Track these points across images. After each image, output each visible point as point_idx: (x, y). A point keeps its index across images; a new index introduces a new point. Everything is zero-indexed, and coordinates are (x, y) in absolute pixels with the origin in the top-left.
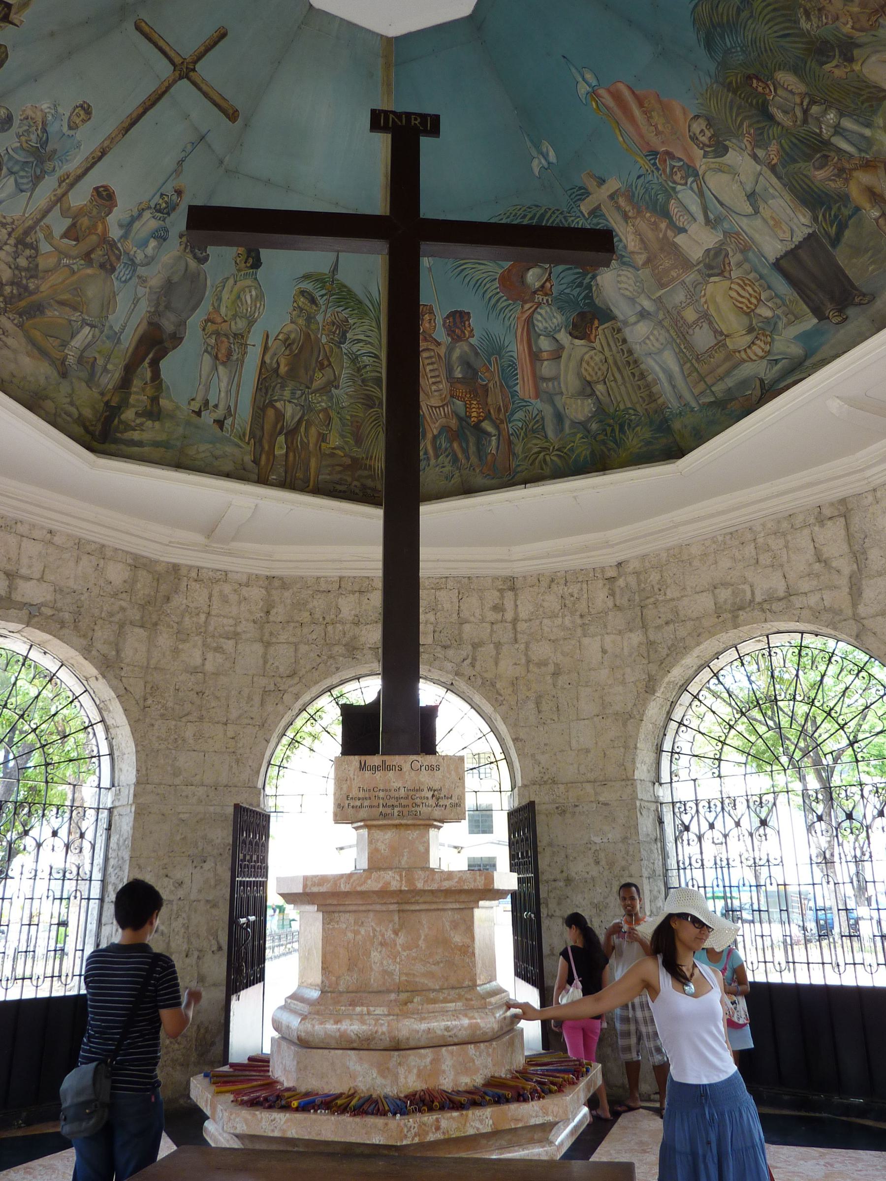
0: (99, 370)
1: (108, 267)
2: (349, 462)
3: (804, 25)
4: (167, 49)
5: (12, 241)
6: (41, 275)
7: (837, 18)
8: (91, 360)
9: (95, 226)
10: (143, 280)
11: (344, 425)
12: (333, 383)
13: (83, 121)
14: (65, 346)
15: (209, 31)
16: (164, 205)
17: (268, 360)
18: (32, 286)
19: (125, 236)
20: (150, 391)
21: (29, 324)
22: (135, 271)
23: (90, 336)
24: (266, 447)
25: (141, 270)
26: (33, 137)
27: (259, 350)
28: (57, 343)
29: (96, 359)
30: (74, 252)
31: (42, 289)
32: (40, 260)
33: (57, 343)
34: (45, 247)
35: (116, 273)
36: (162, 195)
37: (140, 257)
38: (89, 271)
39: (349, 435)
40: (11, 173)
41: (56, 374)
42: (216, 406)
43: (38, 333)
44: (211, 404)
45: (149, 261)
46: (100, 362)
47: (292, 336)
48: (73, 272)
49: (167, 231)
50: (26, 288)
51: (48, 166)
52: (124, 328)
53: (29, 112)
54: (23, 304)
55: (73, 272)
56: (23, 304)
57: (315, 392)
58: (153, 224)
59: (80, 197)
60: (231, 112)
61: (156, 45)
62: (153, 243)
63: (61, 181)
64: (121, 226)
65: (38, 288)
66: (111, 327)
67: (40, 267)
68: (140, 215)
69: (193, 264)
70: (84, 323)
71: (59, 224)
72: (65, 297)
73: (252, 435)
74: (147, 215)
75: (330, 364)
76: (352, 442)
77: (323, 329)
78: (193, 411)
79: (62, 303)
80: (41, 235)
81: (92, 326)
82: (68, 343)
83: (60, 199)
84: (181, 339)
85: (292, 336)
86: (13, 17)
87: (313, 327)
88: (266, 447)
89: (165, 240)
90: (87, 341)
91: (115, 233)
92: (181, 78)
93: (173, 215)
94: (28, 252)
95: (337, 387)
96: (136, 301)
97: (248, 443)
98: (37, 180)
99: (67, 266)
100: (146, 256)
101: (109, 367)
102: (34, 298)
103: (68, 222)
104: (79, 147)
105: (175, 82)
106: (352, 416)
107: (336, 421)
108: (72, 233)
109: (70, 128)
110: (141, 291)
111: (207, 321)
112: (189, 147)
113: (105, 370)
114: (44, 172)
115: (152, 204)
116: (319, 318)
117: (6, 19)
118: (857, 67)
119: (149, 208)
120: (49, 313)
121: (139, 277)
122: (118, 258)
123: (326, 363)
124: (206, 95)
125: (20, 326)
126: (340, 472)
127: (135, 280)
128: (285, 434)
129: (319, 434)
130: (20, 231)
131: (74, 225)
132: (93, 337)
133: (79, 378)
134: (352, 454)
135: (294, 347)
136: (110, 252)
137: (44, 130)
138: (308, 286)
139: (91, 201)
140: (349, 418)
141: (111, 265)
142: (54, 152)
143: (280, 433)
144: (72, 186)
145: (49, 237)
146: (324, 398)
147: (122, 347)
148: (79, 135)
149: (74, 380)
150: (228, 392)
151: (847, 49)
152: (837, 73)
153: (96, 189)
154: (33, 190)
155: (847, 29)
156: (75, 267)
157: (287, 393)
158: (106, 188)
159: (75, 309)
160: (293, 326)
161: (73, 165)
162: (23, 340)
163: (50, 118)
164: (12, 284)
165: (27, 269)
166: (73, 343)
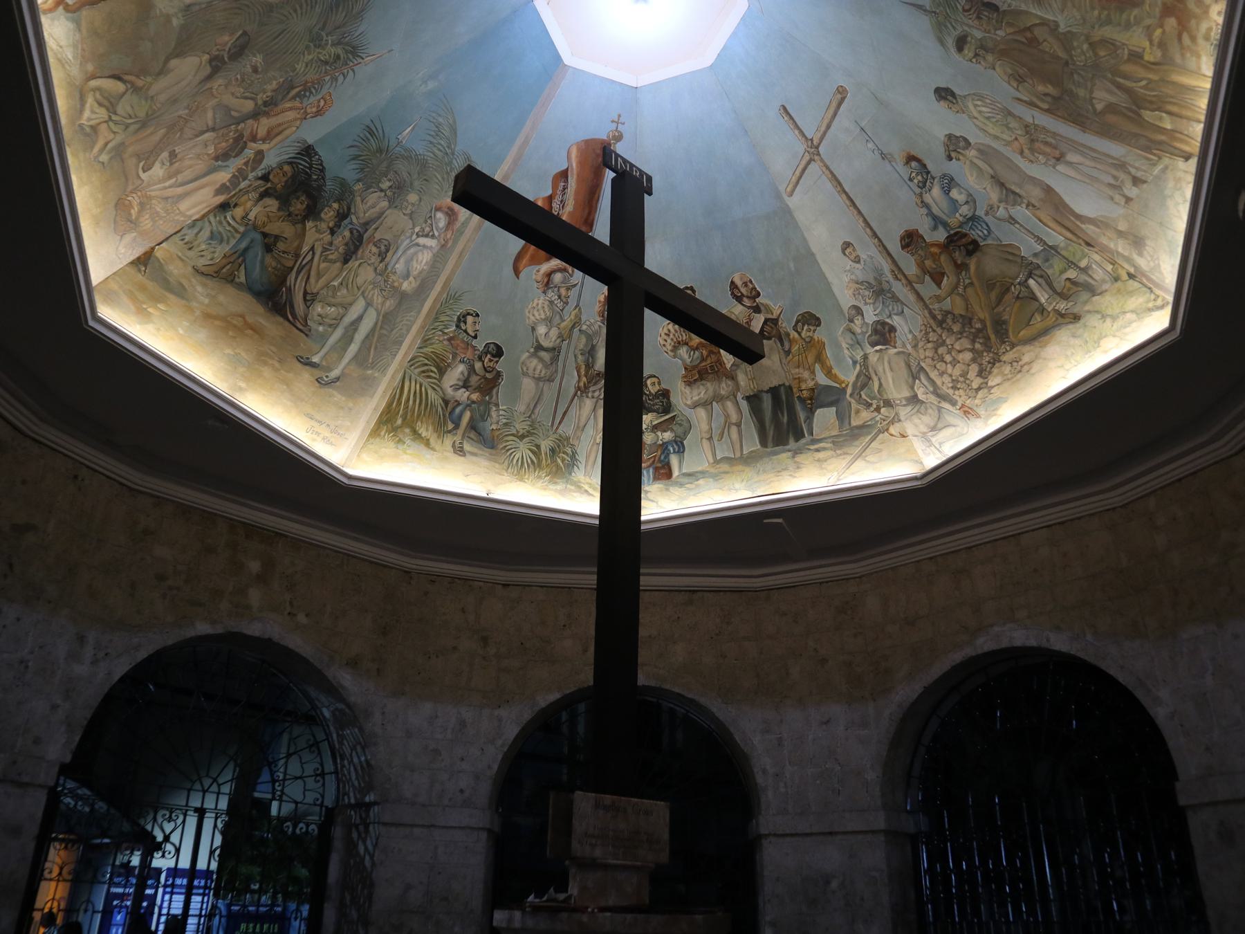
0: (1083, 278)
1: (971, 247)
2: (1171, 22)
3: (258, 59)
4: (801, 167)
5: (939, 330)
6: (969, 315)
7: (226, 86)
8: (1068, 284)
9: (933, 255)
10: (991, 209)
11: (1108, 22)
12: (1053, 28)
13: (854, 250)
14: (1044, 309)
15: (783, 123)
16: (919, 178)
17: (1046, 106)
18: (978, 326)
19: (945, 225)
20: (1109, 233)
21: (1012, 338)
22: (979, 218)
23: (1040, 280)
24: (1163, 138)
25: (980, 213)
26: (867, 293)
27: (1036, 113)
28: (1038, 317)
29: (1068, 279)
30: (953, 279)
31: (982, 316)
32: (956, 312)
33: (1038, 317)
34: (947, 304)
35: (979, 240)
36: (911, 180)
37: (965, 210)
38: (972, 268)
39: (1124, 16)
40: (890, 316)
41: (1071, 326)
42: (1115, 178)
43: (1022, 333)
44: (1112, 182)
45: (971, 200)
46: (1072, 274)
47: (1010, 72)
48: (972, 284)
49: (945, 175)
50: (979, 331)
51: (886, 286)
52: (1039, 240)
53: (851, 292)
54: (993, 337)
55: (972, 284)
56: (993, 337)
57: (1071, 56)
58: (936, 191)
59: (910, 265)
60: (839, 96)
61: (800, 177)
62: (954, 193)
63: (897, 278)
64: (935, 228)
65: (982, 321)
66: (1035, 255)
67: (963, 313)
68: (927, 206)
69: (972, 153)
70: (1024, 284)
71: (928, 289)
72: (993, 295)
73: (1148, 149)
74: (927, 198)
75: (1029, 29)
76: (1136, 12)
77: (989, 32)
78: (1126, 202)
79: (999, 301)
80: (936, 306)
81: (1030, 275)
82: (1041, 305)
83: (910, 283)
84: (1048, 186)
85: (1010, 72)
86: (774, 316)
87: (990, 45)
88: (1163, 138)
89: (952, 179)
90: (1044, 283)
91: (941, 236)
92: (819, 154)
93: (930, 167)
94: (949, 321)
95: (1057, 25)
96: (1012, 220)
97: (1160, 158)
98: (895, 299)
99: (965, 288)
100: (967, 202)
101: (1083, 264)
102: (988, 324)
103: (927, 278)
104: (872, 258)
105: (822, 160)
106: (1093, 8)
107: (1108, 32)
108: (937, 278)
109: (858, 262)
110: (1001, 212)
111: (1022, 153)
112: (870, 145)
113: (1085, 270)
114: (889, 291)
115: (918, 190)
116: (978, 34)
117: (775, 322)
118: (206, 57)
119: (921, 195)
120: (1006, 317)
121: (987, 214)
122: (966, 235)
123: (1029, 35)
124: (828, 127)
125: (1013, 346)
126: (1193, 39)
127: (989, 219)
128: (1140, 108)
129: (1129, 60)
130: (932, 321)
131: (931, 276)
132: (1041, 277)
133: (1086, 302)
134: (1157, 11)
135: (1021, 72)
136: (959, 243)
137: (862, 283)
138: (950, 42)
139: (913, 255)
140: (1096, 13)
141: (970, 244)
142: (875, 279)
143: (1140, 116)
144: (899, 269)
145: (939, 299)
146: (1075, 44)
147: (1062, 245)
148: (863, 256)
149: (1087, 308)
150: (1094, 159)
151: (217, 65)
152: (226, 38)
153: (903, 247)
154: (902, 303)
155: (218, 83)
156: (967, 281)
157: (1081, 92)
158: (902, 239)
159: (1008, 289)
160: (998, 69)
161: (886, 267)
162: (1027, 348)
163: (853, 277)
164: (973, 342)
165: (964, 326)
166: (1043, 300)
